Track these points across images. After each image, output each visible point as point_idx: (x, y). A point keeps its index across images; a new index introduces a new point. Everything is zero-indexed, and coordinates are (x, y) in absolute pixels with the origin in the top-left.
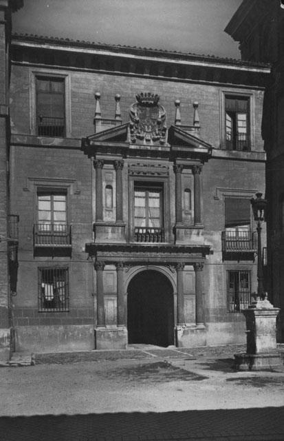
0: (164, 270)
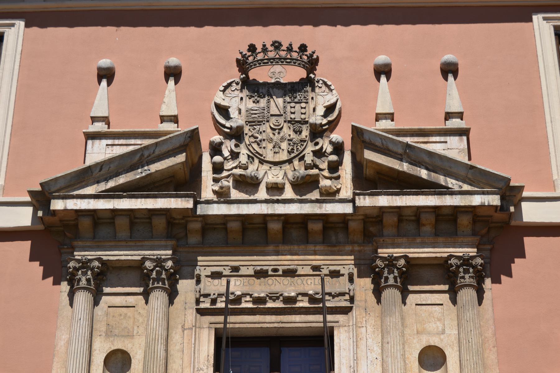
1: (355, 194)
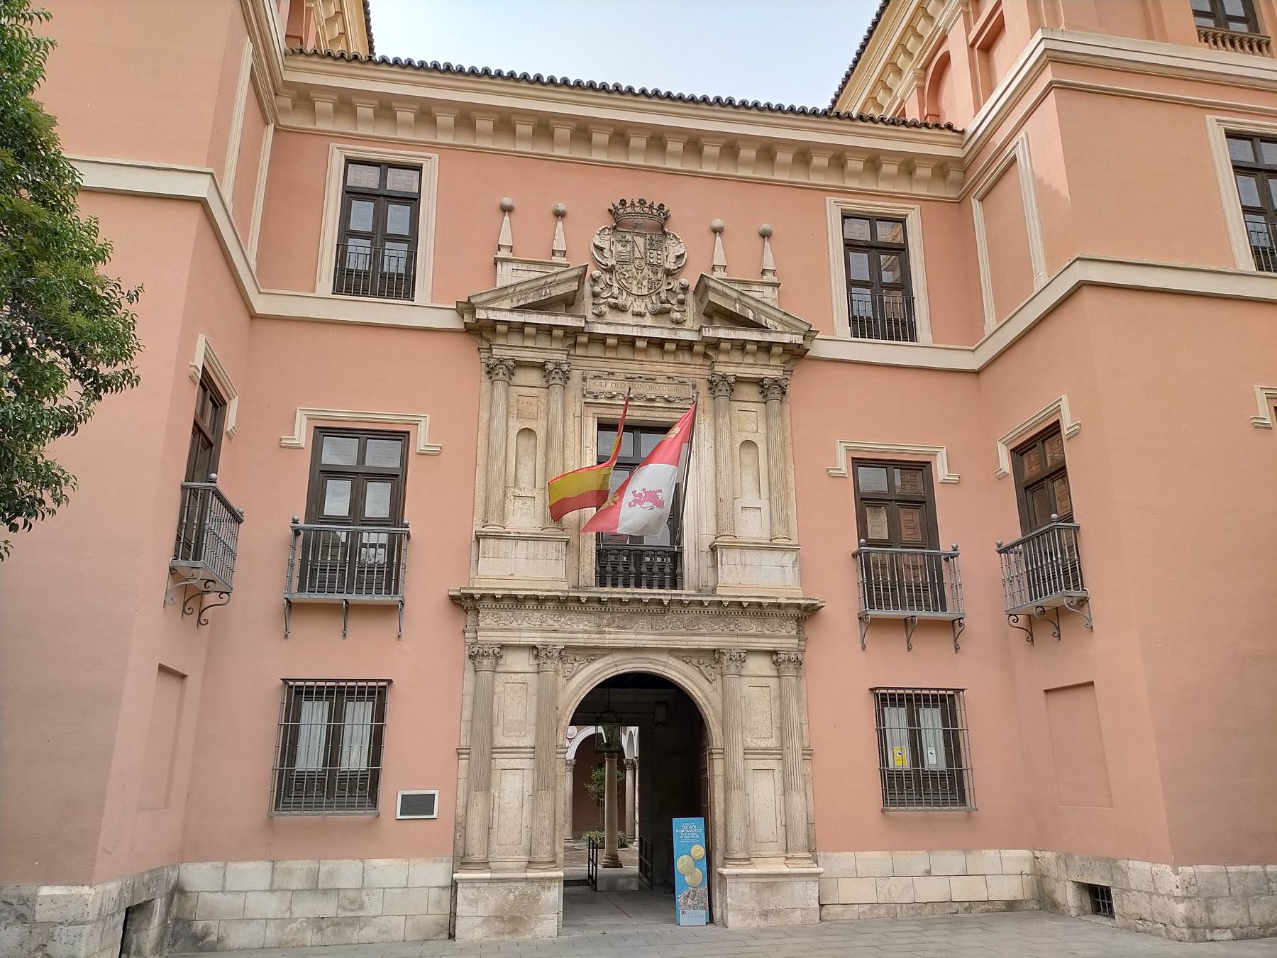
0: (675, 671)
1: (702, 326)
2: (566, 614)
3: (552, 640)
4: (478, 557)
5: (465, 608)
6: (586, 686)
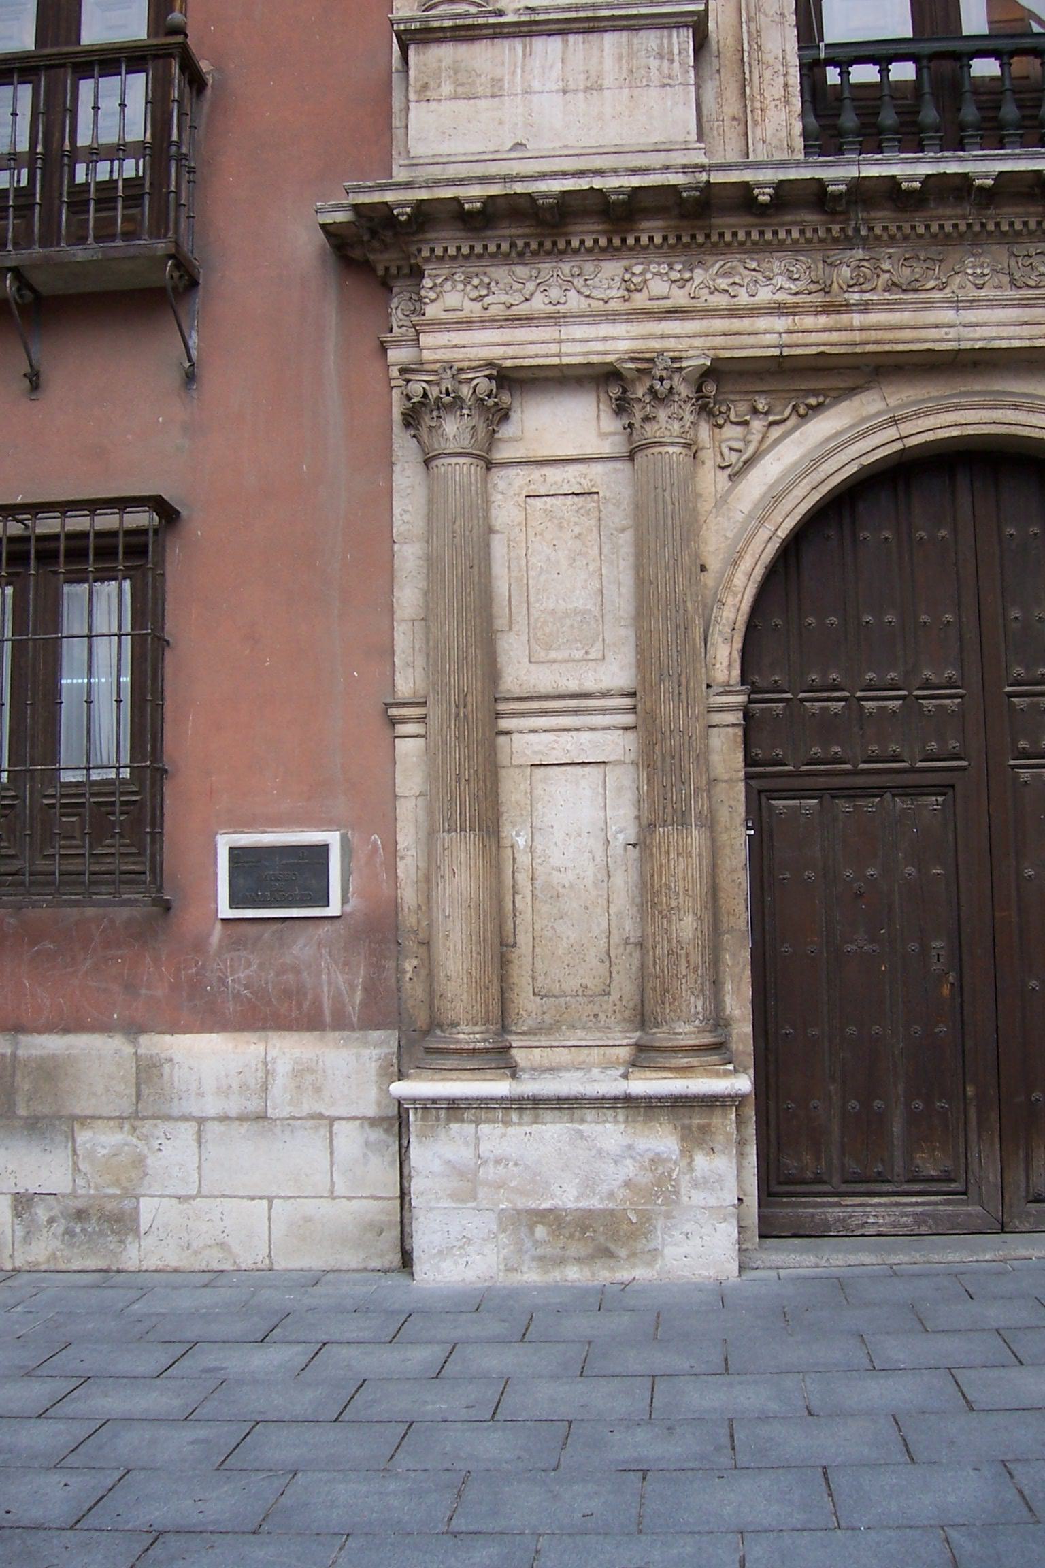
2: (710, 259)
3: (671, 343)
4: (408, 101)
5: (381, 272)
6: (799, 492)
